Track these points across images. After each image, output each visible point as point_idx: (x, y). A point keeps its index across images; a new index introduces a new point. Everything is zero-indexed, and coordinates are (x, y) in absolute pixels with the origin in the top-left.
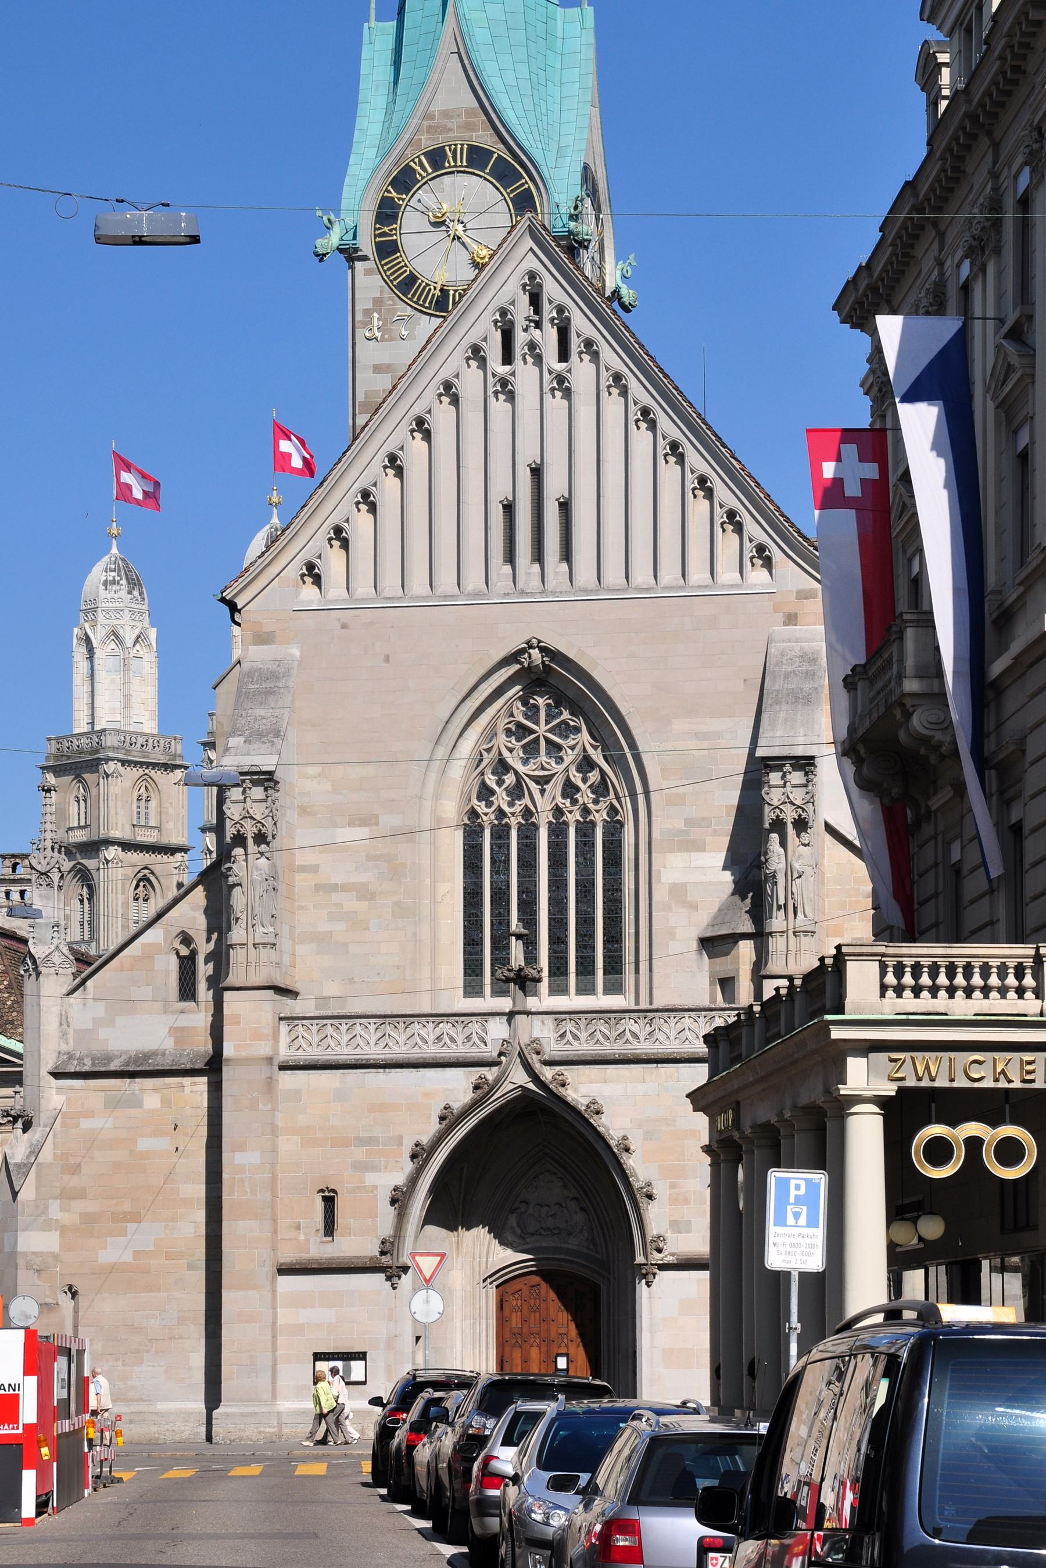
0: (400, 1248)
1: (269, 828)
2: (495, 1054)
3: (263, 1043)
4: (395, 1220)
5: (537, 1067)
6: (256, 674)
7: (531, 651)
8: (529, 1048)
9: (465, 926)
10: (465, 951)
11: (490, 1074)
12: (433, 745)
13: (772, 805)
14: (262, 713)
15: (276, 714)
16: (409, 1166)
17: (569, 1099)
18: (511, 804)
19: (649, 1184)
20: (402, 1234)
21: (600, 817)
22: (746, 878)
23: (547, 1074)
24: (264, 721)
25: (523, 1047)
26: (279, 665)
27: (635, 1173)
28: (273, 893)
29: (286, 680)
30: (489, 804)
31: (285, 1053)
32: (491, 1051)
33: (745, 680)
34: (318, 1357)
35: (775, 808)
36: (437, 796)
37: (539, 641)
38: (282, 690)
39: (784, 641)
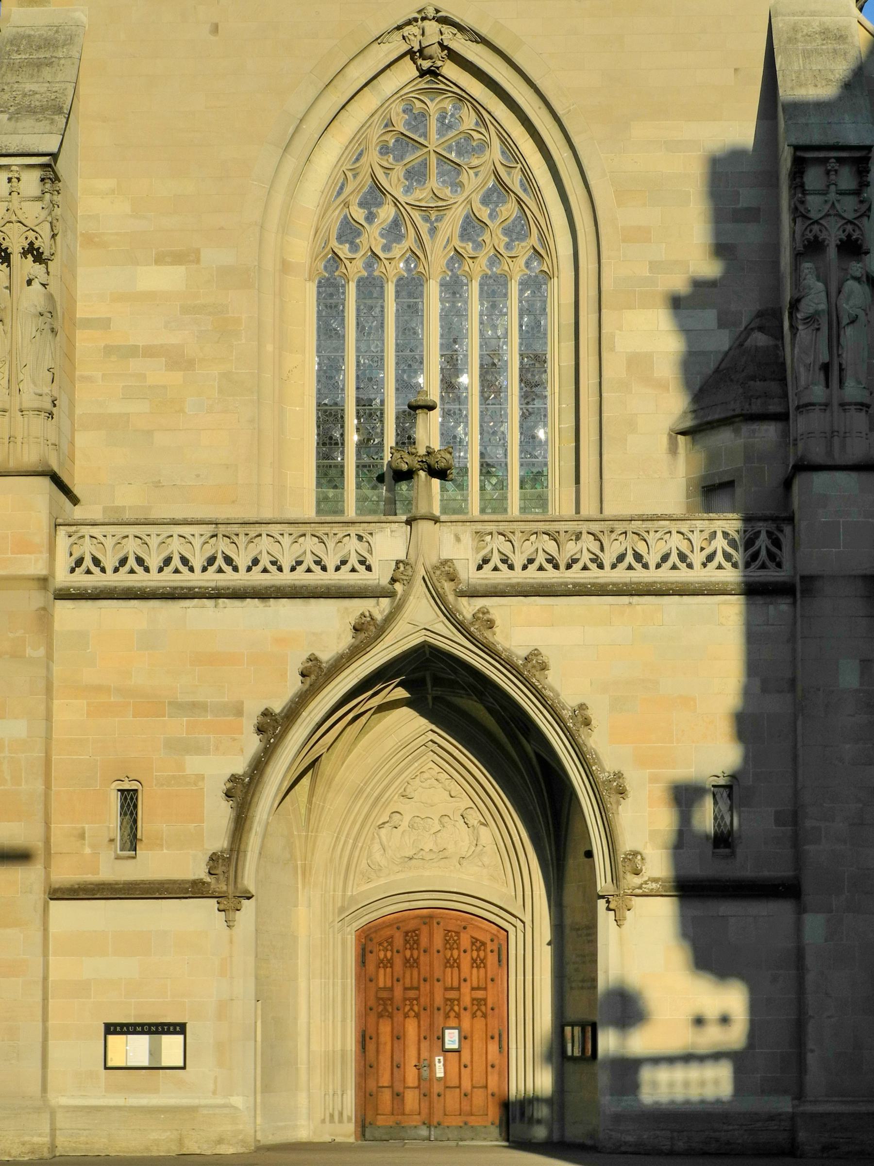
0: (240, 864)
1: (44, 244)
2: (385, 581)
3: (33, 557)
4: (232, 826)
5: (451, 598)
6: (24, 42)
7: (426, 23)
8: (438, 572)
9: (318, 418)
10: (318, 453)
11: (379, 608)
12: (281, 151)
13: (810, 219)
14: (35, 87)
15: (54, 89)
16: (253, 743)
17: (499, 647)
18: (387, 248)
19: (619, 775)
20: (242, 847)
21: (517, 270)
22: (741, 345)
23: (467, 608)
24: (37, 96)
25: (430, 569)
26: (57, 32)
27: (598, 759)
28: (50, 336)
29: (68, 50)
30: (354, 248)
31: (63, 578)
32: (380, 576)
33: (736, 70)
34: (112, 1029)
35: (813, 223)
36: (285, 228)
37: (437, 11)
38: (62, 61)
39: (794, 15)
